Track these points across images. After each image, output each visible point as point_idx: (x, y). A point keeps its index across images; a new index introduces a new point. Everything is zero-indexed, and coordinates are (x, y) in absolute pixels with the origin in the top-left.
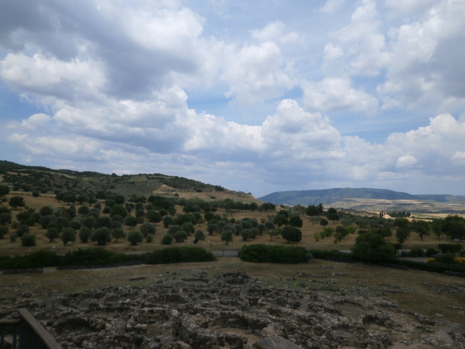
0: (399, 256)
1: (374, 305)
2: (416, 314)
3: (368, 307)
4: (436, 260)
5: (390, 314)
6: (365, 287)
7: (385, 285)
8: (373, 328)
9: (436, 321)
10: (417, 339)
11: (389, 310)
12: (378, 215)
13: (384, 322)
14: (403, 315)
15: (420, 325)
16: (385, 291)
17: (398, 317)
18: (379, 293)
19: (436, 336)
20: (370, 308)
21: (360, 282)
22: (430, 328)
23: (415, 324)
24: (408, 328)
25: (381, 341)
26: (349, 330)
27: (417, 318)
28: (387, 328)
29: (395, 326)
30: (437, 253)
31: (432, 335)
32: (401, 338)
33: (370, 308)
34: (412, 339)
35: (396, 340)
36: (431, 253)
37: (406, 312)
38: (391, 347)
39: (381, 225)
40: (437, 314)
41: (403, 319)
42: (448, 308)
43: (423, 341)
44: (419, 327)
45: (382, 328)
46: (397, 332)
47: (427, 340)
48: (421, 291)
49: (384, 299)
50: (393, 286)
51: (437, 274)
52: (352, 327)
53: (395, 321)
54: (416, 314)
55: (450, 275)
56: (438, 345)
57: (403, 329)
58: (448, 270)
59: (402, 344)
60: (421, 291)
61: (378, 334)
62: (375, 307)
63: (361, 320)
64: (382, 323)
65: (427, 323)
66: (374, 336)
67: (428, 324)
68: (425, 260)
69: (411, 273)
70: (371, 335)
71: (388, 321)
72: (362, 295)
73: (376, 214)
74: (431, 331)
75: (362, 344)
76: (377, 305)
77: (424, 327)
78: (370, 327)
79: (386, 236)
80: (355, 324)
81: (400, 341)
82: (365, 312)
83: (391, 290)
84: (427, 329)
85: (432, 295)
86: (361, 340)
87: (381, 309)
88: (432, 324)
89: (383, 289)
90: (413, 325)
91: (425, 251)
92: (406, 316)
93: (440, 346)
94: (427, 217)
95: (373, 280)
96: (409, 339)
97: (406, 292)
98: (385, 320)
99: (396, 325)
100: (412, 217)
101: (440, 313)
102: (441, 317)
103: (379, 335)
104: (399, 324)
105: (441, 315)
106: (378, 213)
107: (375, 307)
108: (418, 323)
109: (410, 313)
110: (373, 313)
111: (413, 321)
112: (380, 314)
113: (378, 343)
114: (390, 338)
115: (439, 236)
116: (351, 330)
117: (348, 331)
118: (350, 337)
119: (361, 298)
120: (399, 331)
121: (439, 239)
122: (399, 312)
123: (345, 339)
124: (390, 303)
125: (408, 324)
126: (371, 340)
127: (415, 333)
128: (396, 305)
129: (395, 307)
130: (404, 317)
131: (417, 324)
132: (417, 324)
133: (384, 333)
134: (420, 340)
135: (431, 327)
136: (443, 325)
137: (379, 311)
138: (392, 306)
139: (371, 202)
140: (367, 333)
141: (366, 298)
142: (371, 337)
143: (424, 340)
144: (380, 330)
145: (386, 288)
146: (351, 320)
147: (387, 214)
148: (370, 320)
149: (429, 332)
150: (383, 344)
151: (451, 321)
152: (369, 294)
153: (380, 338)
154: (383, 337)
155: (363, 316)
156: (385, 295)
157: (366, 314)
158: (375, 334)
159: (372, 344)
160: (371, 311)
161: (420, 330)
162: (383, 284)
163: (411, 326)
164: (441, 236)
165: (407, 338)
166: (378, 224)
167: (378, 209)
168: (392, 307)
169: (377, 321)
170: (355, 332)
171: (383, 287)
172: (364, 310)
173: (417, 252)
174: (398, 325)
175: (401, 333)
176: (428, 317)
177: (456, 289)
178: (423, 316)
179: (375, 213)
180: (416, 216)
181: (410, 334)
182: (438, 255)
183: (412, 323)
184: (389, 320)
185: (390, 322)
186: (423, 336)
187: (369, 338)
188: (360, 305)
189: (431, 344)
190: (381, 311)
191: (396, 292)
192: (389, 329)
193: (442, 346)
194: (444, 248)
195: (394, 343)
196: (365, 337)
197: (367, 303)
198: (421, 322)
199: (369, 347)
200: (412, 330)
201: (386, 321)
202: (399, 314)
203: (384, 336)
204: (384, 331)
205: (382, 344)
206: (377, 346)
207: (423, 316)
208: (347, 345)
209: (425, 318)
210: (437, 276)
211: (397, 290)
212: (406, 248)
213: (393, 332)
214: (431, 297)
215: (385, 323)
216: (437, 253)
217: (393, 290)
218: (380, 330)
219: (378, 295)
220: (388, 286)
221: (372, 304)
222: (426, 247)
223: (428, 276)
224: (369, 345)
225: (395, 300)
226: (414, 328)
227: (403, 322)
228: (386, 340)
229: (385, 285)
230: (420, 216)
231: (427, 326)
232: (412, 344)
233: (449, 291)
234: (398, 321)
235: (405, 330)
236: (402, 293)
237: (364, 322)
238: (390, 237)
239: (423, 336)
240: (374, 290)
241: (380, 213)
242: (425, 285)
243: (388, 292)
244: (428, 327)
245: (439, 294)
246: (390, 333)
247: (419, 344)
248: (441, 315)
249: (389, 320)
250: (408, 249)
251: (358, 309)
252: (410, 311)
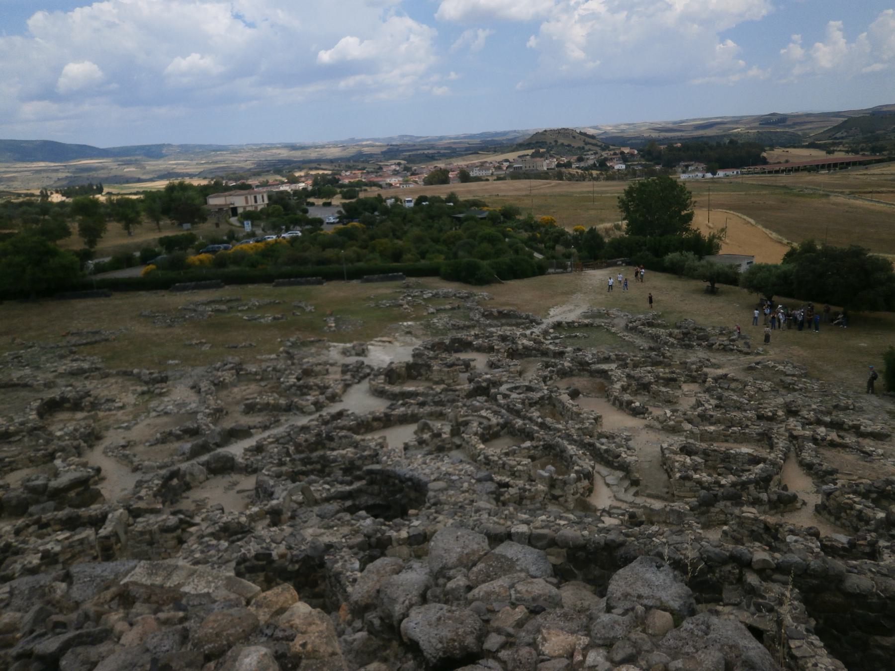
0: (90, 274)
1: (56, 377)
2: (136, 371)
3: (45, 385)
4: (158, 268)
5: (90, 385)
6: (31, 347)
7: (72, 334)
8: (61, 421)
9: (170, 373)
10: (144, 412)
11: (86, 378)
12: (38, 196)
13: (81, 403)
14: (113, 380)
15: (145, 388)
16: (74, 345)
17: (106, 385)
18: (63, 352)
19: (173, 398)
20: (49, 385)
21: (18, 341)
22: (162, 388)
23: (136, 390)
24: (125, 400)
25: (81, 438)
26: (12, 439)
27: (138, 378)
28: (89, 412)
29: (101, 404)
30: (159, 254)
31: (166, 399)
32: (117, 421)
33: (49, 385)
34: (136, 417)
35: (107, 428)
36: (148, 256)
37: (118, 374)
38: (101, 442)
39: (47, 217)
40: (170, 362)
41: (114, 386)
42: (185, 346)
43: (154, 414)
44: (143, 393)
45: (79, 415)
46: (107, 413)
47: (159, 409)
48: (139, 329)
49: (73, 361)
50: (88, 333)
51: (163, 292)
52: (16, 433)
53: (102, 394)
54: (136, 371)
55: (184, 289)
56: (178, 412)
57: (117, 405)
58: (179, 282)
59: (120, 430)
60: (139, 329)
61: (71, 428)
62: (58, 381)
63: (34, 412)
64: (76, 406)
65: (155, 381)
66: (66, 434)
67: (158, 382)
68: (138, 272)
69: (118, 301)
70: (59, 434)
71: (88, 399)
72: (27, 365)
73: (32, 195)
74: (165, 392)
75: (44, 456)
76: (61, 375)
77: (152, 389)
78: (55, 420)
79: (61, 237)
80: (22, 424)
81: (116, 426)
82: (40, 395)
83: (85, 341)
84: (157, 391)
85: (158, 331)
86: (42, 450)
87: (72, 381)
88: (164, 380)
89: (68, 342)
90: (134, 392)
91: (137, 254)
92: (120, 380)
93: (181, 412)
94: (134, 191)
95: (46, 331)
96: (131, 417)
97: (113, 337)
98: (82, 398)
99: (103, 401)
100: (109, 193)
101: (174, 358)
102: (177, 364)
103: (76, 430)
104: (109, 398)
105: (177, 362)
106: (37, 192)
107: (58, 381)
108: (141, 386)
109: (127, 374)
110: (54, 394)
111: (133, 385)
112: (70, 391)
113: (75, 443)
114: (97, 427)
115: (158, 224)
116: (17, 438)
117: (10, 443)
118: (16, 453)
119: (28, 371)
120: (110, 410)
121: (159, 229)
122: (107, 376)
123: (7, 460)
124: (86, 365)
125: (124, 394)
126: (61, 443)
127: (138, 405)
128: (98, 366)
129: (97, 369)
130: (116, 383)
131: (140, 389)
132: (140, 389)
133: (83, 423)
134: (149, 413)
135: (164, 385)
136: (182, 376)
137: (67, 386)
138: (91, 370)
139: (15, 170)
140: (51, 434)
141: (38, 368)
142: (60, 438)
143: (155, 410)
144: (76, 420)
145: (74, 340)
146: (12, 419)
147: (57, 192)
148: (51, 407)
149: (161, 395)
150: (85, 442)
151: (193, 366)
152: (44, 358)
153: (77, 434)
154: (82, 430)
155: (36, 404)
156: (74, 353)
157: (42, 399)
158: (66, 430)
159: (63, 449)
160: (51, 390)
161: (147, 397)
162: (68, 334)
163: (130, 395)
164: (161, 223)
165: (126, 418)
166: (37, 216)
167: (36, 184)
168: (93, 372)
169: (67, 405)
170: (26, 439)
171: (69, 338)
172: (38, 391)
173: (124, 260)
174: (108, 400)
175: (114, 412)
176: (156, 371)
177: (195, 311)
178: (148, 372)
179: (29, 192)
180: (114, 191)
181: (130, 409)
182: (159, 258)
183: (131, 388)
184: (90, 396)
185: (91, 399)
186: (152, 406)
187: (55, 441)
188: (25, 385)
189: (166, 413)
190: (71, 385)
191: (96, 342)
192: (93, 413)
193: (183, 411)
194: (168, 244)
195: (104, 433)
196: (48, 442)
197: (41, 377)
198: (147, 383)
199: (60, 457)
200: (133, 401)
201: (83, 400)
202: (106, 380)
203: (85, 428)
204: (84, 419)
205: (83, 444)
206: (74, 450)
207: (148, 372)
208: (12, 470)
209: (151, 374)
210: (163, 296)
211: (97, 338)
212: (102, 256)
213: (101, 414)
214: (157, 335)
215: (83, 404)
216: (159, 254)
217: (89, 340)
218: (76, 420)
219: (62, 357)
220: (78, 334)
221: (50, 376)
222: (138, 247)
223: (148, 300)
224: (59, 454)
225: (95, 357)
226: (135, 396)
227: (116, 392)
228: (90, 434)
229: (72, 334)
230: (122, 189)
231: (156, 386)
232: (136, 424)
233: (184, 317)
234: (106, 392)
235: (120, 404)
236: (107, 340)
237: (41, 414)
238: (67, 239)
239: (153, 404)
240: (52, 348)
241: (42, 192)
242: (145, 316)
243: (80, 345)
244: (158, 388)
245: (170, 326)
246: (96, 419)
247: (148, 421)
248: (177, 362)
249: (90, 396)
250: (108, 256)
251: (23, 393)
252: (124, 369)
